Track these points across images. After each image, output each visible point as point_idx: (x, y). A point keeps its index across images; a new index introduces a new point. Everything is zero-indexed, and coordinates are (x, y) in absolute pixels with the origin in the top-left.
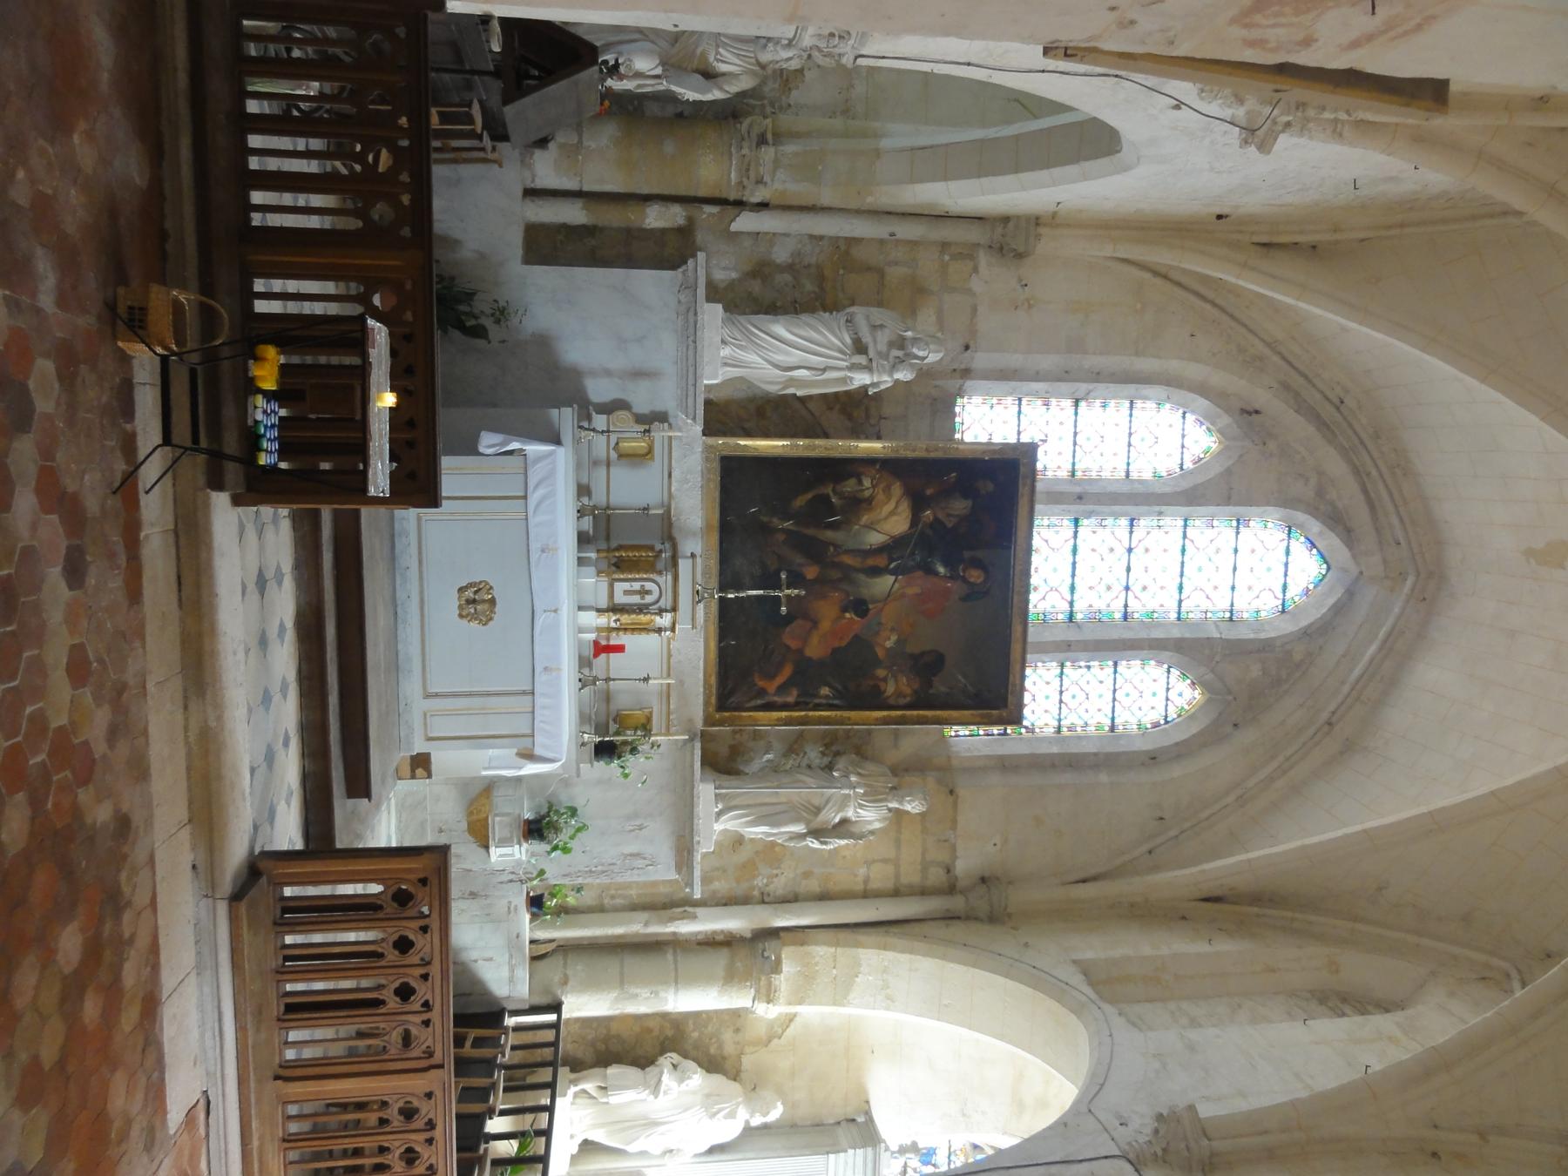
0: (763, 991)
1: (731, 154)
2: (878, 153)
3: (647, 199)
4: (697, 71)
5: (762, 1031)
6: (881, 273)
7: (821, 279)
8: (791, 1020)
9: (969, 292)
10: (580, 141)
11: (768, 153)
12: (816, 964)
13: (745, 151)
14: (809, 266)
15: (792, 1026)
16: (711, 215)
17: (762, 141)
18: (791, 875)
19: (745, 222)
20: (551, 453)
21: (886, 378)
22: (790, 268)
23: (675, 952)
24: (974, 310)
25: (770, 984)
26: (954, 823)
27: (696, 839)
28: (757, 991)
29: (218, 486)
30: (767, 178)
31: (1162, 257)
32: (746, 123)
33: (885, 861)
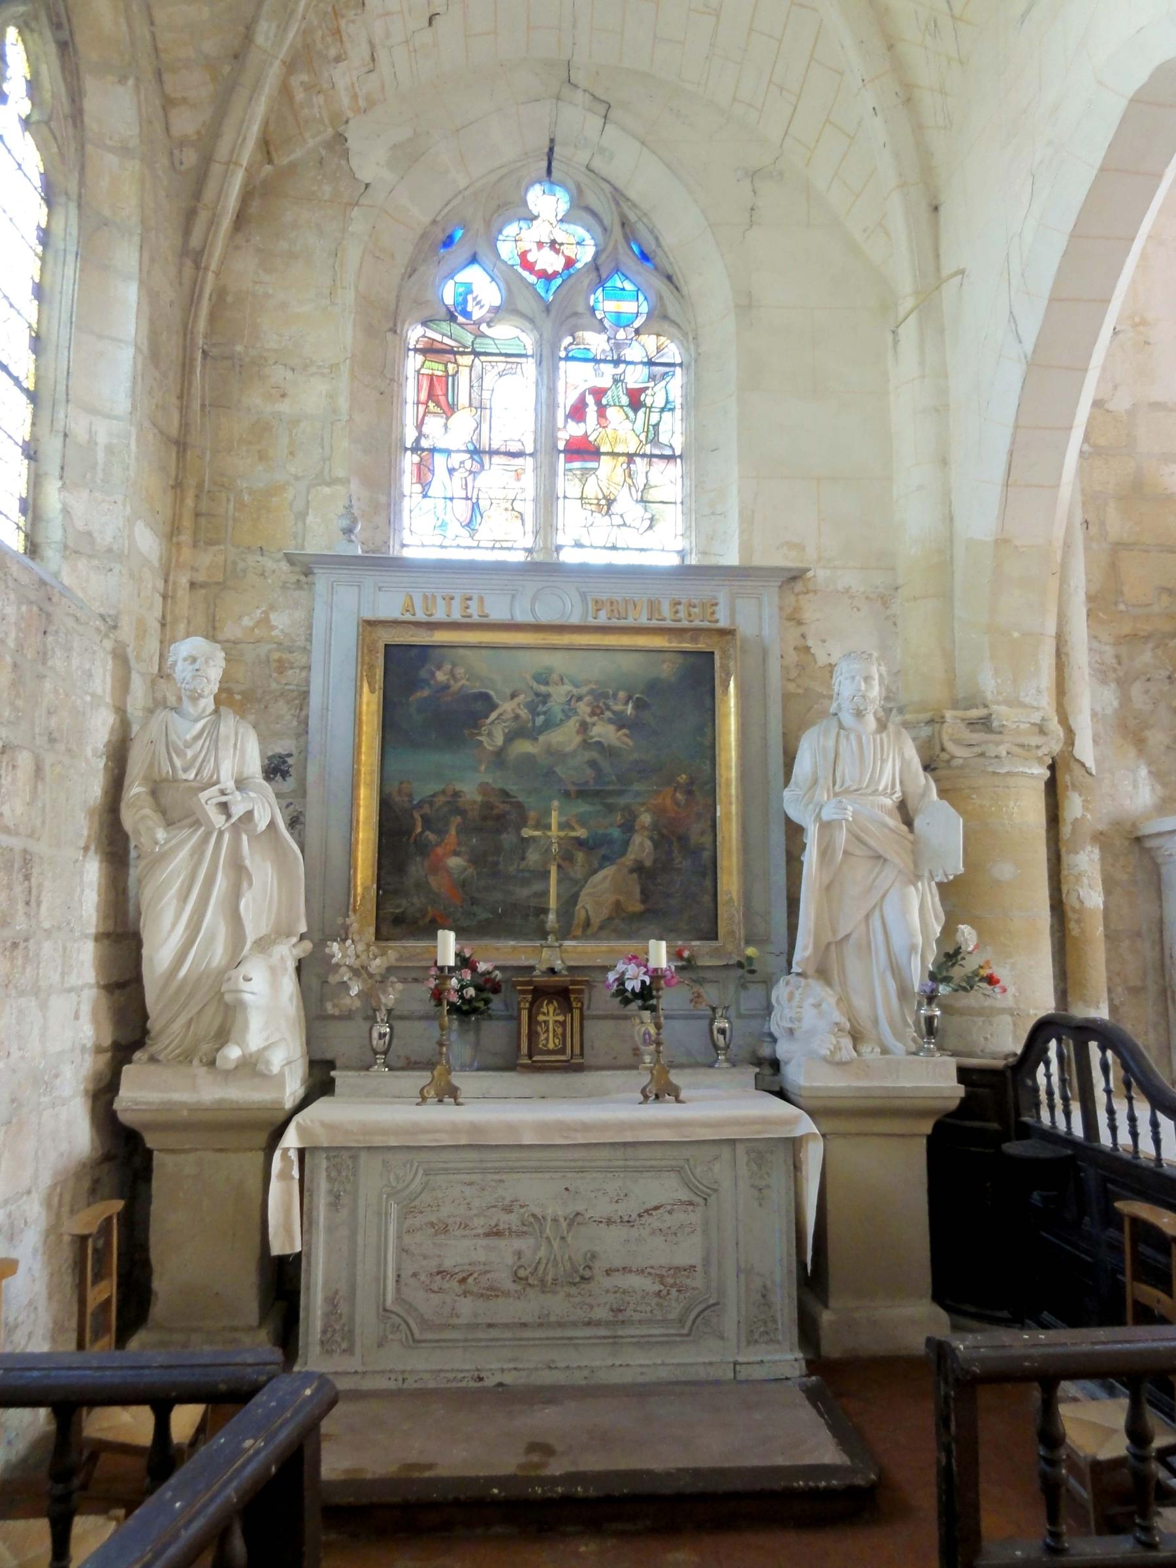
1: (1008, 774)
2: (1001, 542)
3: (1058, 907)
4: (909, 822)
6: (1118, 547)
7: (1133, 638)
9: (1132, 412)
10: (1010, 1012)
11: (1003, 714)
13: (1002, 750)
14: (1118, 657)
16: (1085, 808)
17: (984, 724)
19: (1085, 751)
22: (1123, 684)
24: (1156, 406)
30: (1036, 718)
32: (949, 746)
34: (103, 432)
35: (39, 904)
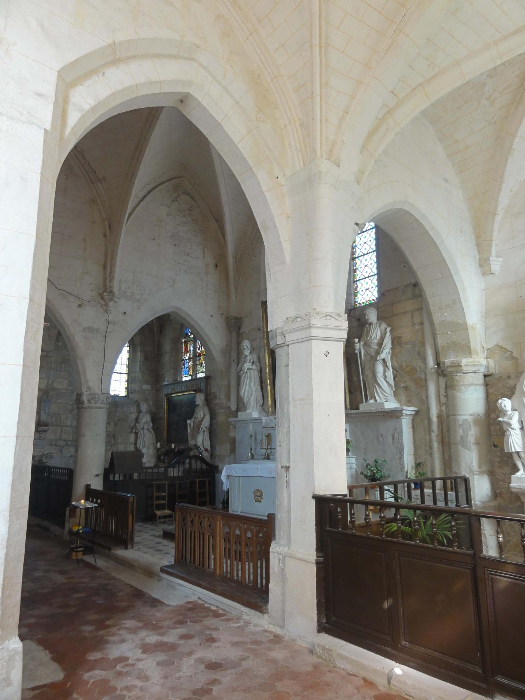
0: (456, 369)
5: (508, 364)
8: (502, 348)
12: (448, 343)
15: (504, 346)
18: (420, 361)
20: (226, 468)
21: (248, 358)
23: (459, 415)
24: (252, 329)
25: (451, 366)
26: (397, 288)
27: (380, 410)
28: (457, 372)
29: (110, 549)
31: (231, 275)
33: (412, 317)
34: (137, 374)
35: (118, 440)
